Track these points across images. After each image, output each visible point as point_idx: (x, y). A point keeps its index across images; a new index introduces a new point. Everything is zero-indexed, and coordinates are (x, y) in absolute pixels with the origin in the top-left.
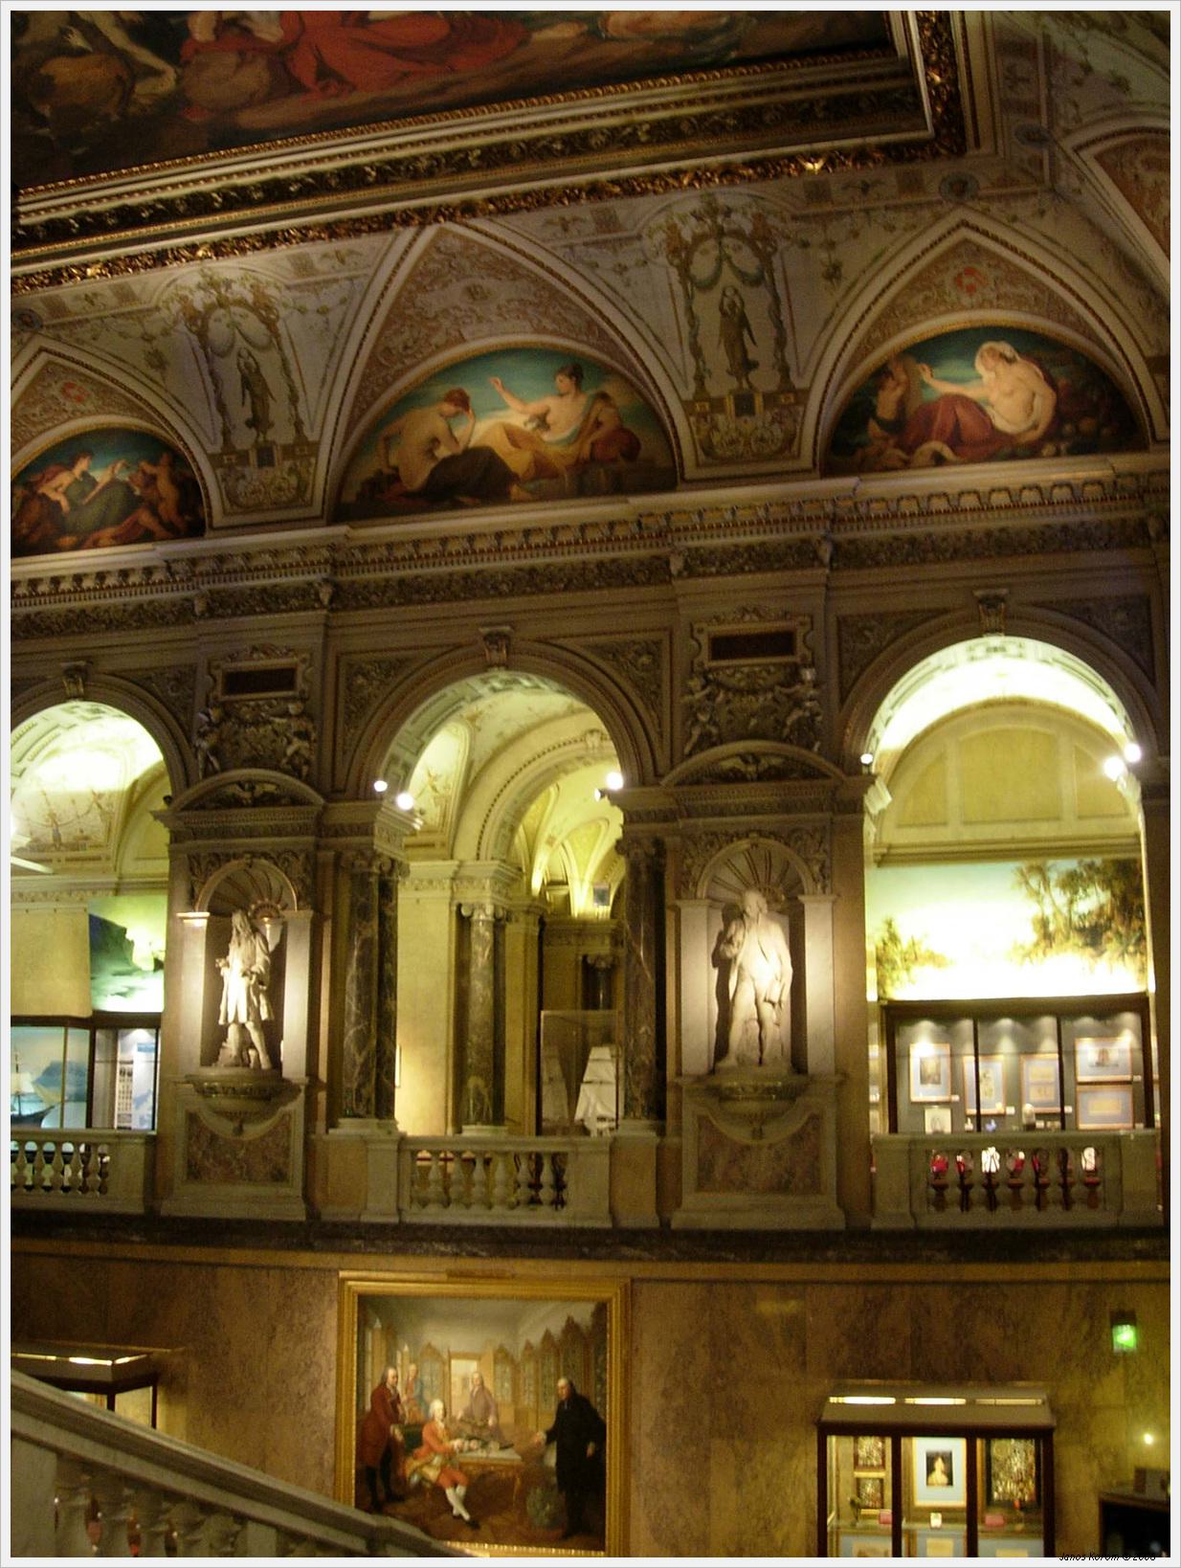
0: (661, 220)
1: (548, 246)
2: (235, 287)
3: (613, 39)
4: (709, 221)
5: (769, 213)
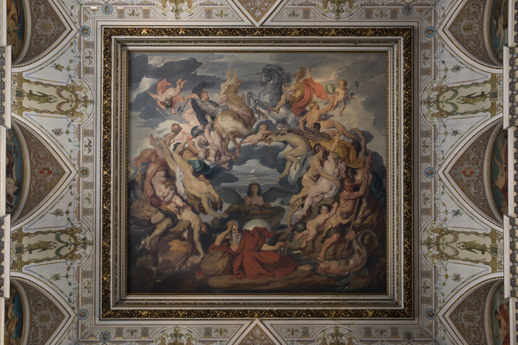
0: (321, 335)
1: (286, 340)
2: (183, 338)
3: (318, 274)
4: (335, 338)
5: (353, 338)
